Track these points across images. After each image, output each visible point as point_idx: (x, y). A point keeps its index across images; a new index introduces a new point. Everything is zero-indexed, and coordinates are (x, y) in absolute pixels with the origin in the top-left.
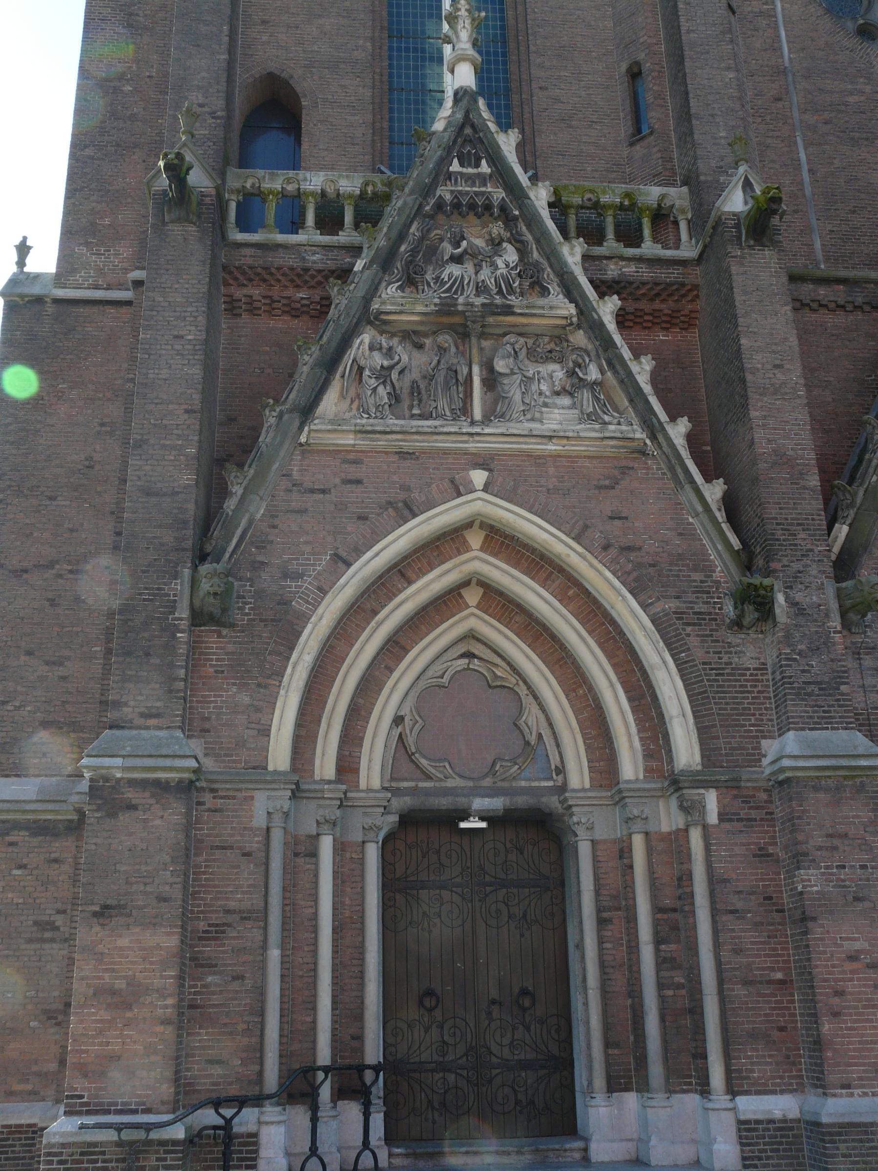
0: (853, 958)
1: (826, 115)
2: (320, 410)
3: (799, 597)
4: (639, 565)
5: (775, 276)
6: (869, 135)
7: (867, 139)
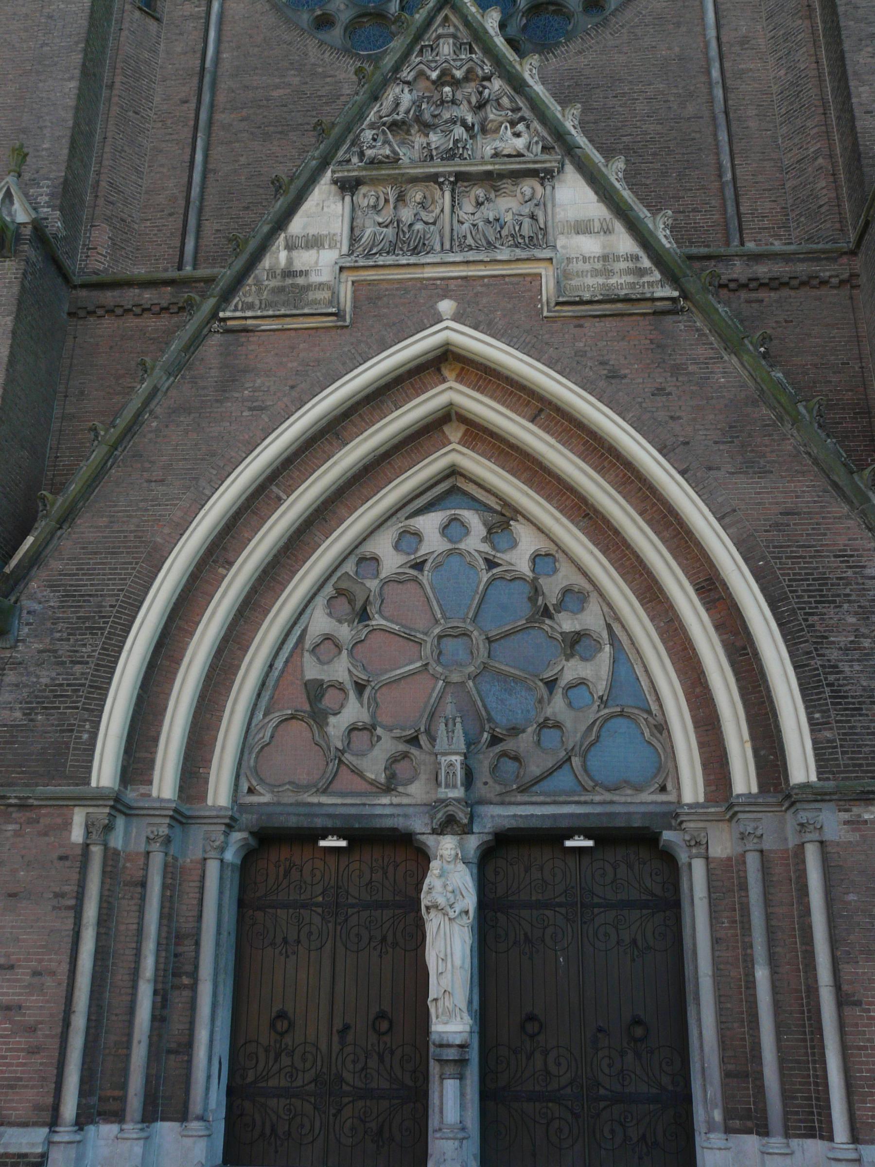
1: (244, 112)
5: (6, 287)
6: (285, 127)
7: (281, 133)
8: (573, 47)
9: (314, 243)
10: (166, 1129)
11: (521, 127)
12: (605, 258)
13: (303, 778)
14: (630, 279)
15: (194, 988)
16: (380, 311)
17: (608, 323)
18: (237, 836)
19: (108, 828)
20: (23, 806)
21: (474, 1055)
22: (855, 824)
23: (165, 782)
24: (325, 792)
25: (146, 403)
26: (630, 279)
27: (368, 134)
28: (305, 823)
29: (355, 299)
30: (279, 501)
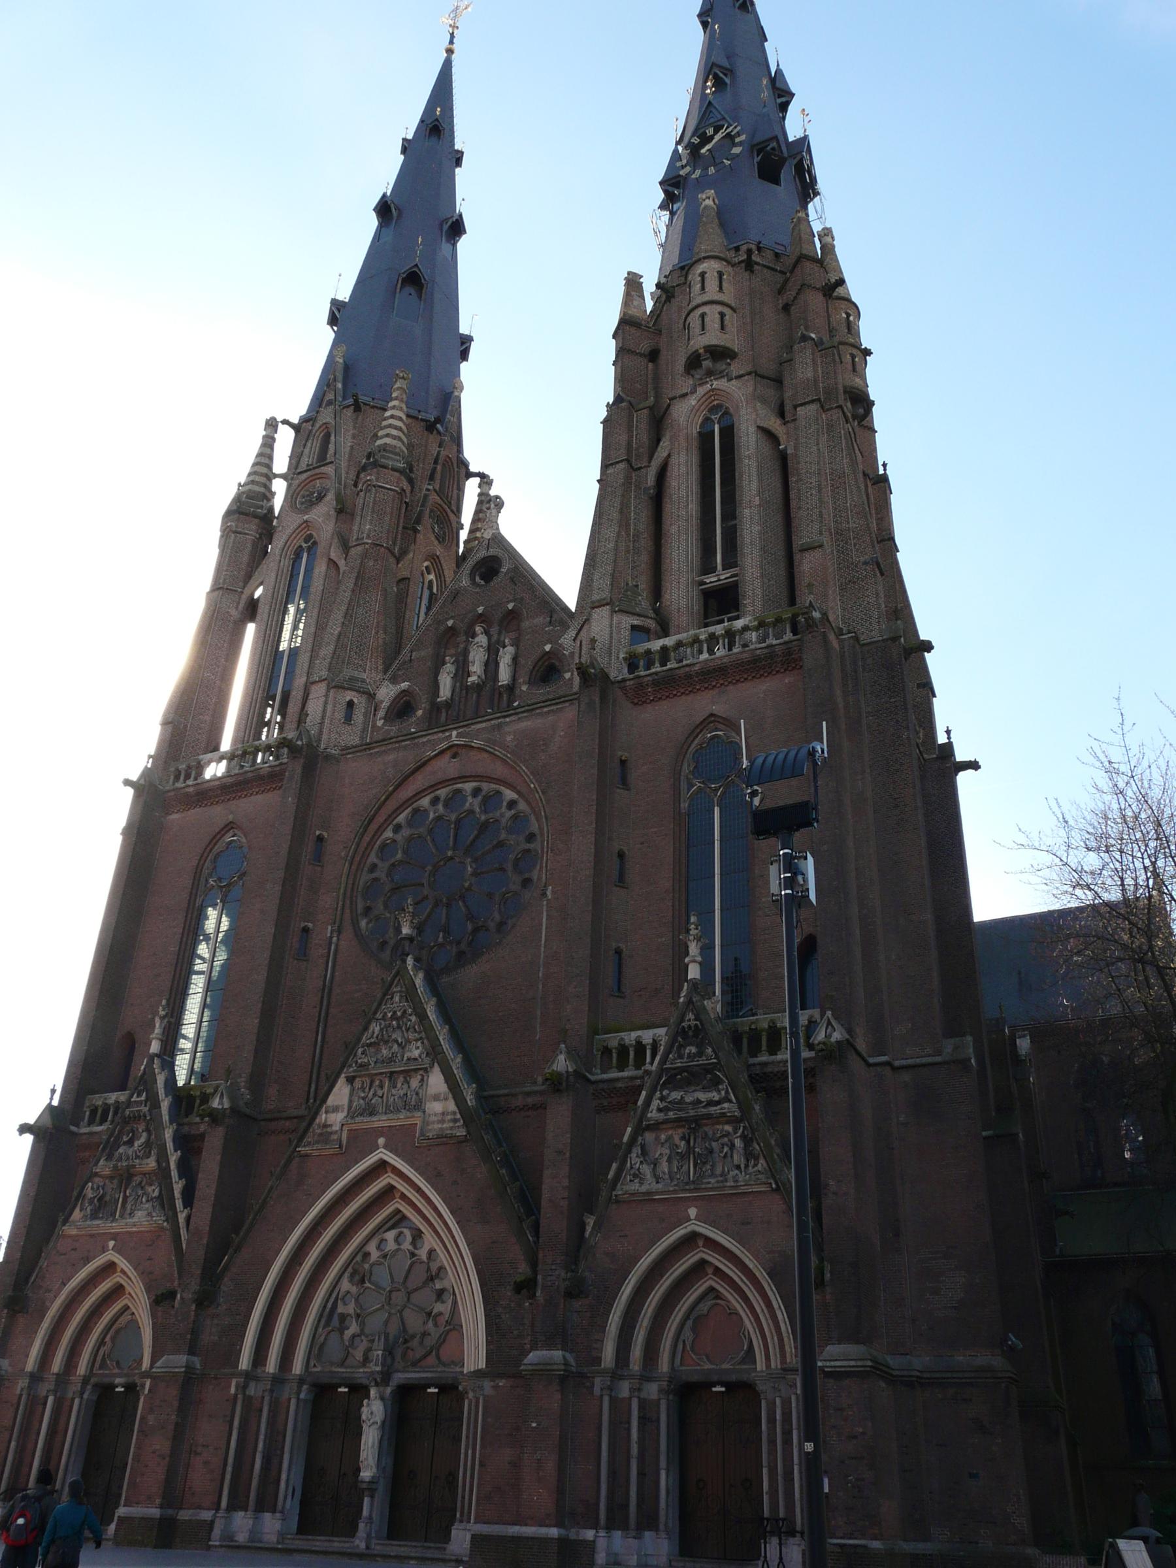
0: (154, 1452)
2: (72, 1218)
3: (185, 1295)
9: (336, 1109)
10: (267, 1516)
11: (419, 1043)
12: (443, 1114)
16: (360, 1142)
18: (305, 1387)
20: (216, 1378)
21: (381, 1488)
22: (496, 1387)
25: (269, 1191)
27: (360, 1050)
29: (348, 1138)
30: (321, 1234)
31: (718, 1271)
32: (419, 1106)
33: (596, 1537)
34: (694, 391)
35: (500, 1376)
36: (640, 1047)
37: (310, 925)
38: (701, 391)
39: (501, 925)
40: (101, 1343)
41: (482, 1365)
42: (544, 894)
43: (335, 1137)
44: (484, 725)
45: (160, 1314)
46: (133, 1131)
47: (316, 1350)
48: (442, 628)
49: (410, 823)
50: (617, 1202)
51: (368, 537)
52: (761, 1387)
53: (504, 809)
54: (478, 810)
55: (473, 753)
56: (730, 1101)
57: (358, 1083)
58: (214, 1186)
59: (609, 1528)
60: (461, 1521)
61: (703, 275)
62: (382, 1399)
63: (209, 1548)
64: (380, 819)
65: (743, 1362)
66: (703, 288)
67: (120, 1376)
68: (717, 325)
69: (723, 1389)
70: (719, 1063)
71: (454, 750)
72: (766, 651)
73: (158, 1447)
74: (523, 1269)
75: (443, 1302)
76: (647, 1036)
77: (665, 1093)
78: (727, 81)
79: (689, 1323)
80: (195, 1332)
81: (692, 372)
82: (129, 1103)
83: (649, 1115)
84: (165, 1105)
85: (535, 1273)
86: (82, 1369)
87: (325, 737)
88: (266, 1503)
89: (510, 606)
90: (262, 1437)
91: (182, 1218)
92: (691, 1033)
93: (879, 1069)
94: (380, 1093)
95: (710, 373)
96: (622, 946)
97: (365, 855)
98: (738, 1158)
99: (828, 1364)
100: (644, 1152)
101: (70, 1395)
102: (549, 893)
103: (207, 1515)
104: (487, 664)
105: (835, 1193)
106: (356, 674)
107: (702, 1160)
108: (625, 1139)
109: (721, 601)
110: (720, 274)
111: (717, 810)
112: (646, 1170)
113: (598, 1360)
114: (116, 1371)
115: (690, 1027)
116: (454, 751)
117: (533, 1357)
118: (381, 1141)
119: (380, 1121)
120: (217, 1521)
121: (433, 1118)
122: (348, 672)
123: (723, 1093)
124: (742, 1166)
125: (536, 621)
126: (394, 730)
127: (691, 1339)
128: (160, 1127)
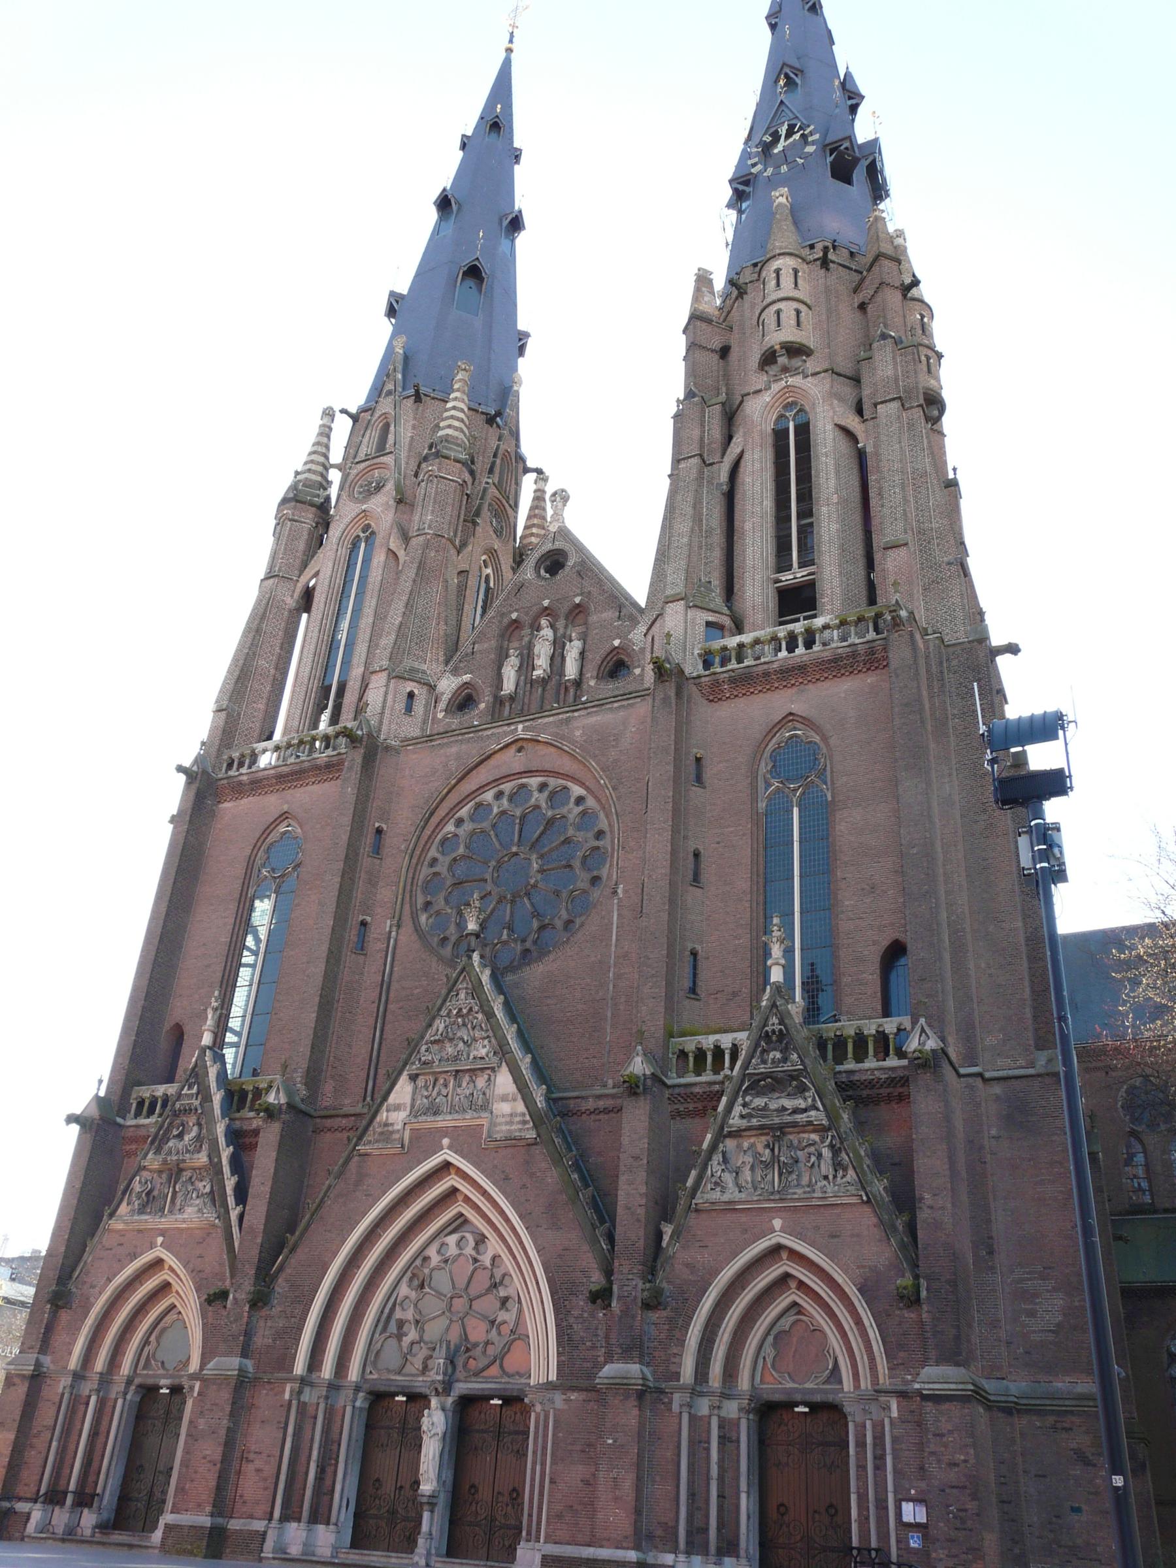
0: (204, 1458)
2: (118, 1213)
3: (237, 1295)
4: (201, 1279)
8: (552, 957)
9: (397, 1108)
10: (321, 1528)
11: (486, 1042)
12: (511, 1115)
13: (391, 1368)
14: (520, 1126)
15: (336, 1465)
16: (423, 1143)
17: (510, 1150)
18: (361, 1395)
19: (300, 1392)
21: (442, 1501)
22: (567, 1401)
23: (327, 1370)
24: (399, 1373)
25: (327, 1191)
26: (520, 1126)
27: (424, 1048)
28: (387, 1389)
30: (380, 1236)
31: (801, 1285)
32: (485, 1107)
33: (675, 1561)
34: (768, 388)
35: (573, 1389)
36: (718, 1052)
37: (368, 919)
38: (776, 387)
39: (569, 923)
40: (146, 1342)
41: (553, 1377)
42: (615, 892)
43: (396, 1136)
44: (551, 719)
45: (210, 1314)
46: (183, 1125)
47: (372, 1357)
48: (506, 621)
49: (472, 818)
50: (697, 1211)
51: (430, 527)
52: (848, 1409)
53: (571, 804)
54: (544, 805)
55: (540, 747)
56: (817, 1109)
57: (421, 1082)
58: (269, 1184)
59: (688, 1553)
60: (528, 1541)
61: (778, 272)
62: (443, 1409)
63: (261, 1559)
64: (441, 812)
65: (827, 1382)
66: (778, 284)
67: (164, 1377)
68: (793, 322)
69: (807, 1410)
70: (805, 1069)
71: (519, 744)
72: (848, 650)
73: (208, 1452)
74: (597, 1279)
75: (507, 1310)
76: (726, 1041)
77: (748, 1099)
78: (798, 80)
79: (770, 1339)
80: (248, 1334)
81: (766, 368)
82: (179, 1096)
83: (731, 1121)
84: (217, 1097)
85: (610, 1283)
86: (126, 1368)
87: (384, 728)
88: (319, 1515)
89: (577, 600)
90: (316, 1446)
91: (234, 1215)
92: (774, 1038)
93: (970, 1080)
94: (444, 1092)
95: (785, 370)
96: (698, 947)
97: (426, 849)
98: (826, 1168)
99: (926, 1386)
100: (725, 1160)
101: (113, 1396)
102: (620, 891)
103: (259, 1525)
104: (552, 658)
105: (931, 1207)
106: (416, 665)
107: (785, 1170)
108: (705, 1146)
109: (796, 600)
110: (796, 271)
111: (796, 810)
112: (728, 1178)
113: (677, 1376)
114: (161, 1372)
115: (773, 1031)
116: (519, 745)
117: (609, 1370)
118: (446, 1141)
119: (444, 1121)
120: (270, 1532)
121: (500, 1120)
122: (408, 663)
123: (810, 1100)
124: (831, 1177)
125: (605, 615)
126: (455, 722)
127: (771, 1356)
128: (212, 1121)
